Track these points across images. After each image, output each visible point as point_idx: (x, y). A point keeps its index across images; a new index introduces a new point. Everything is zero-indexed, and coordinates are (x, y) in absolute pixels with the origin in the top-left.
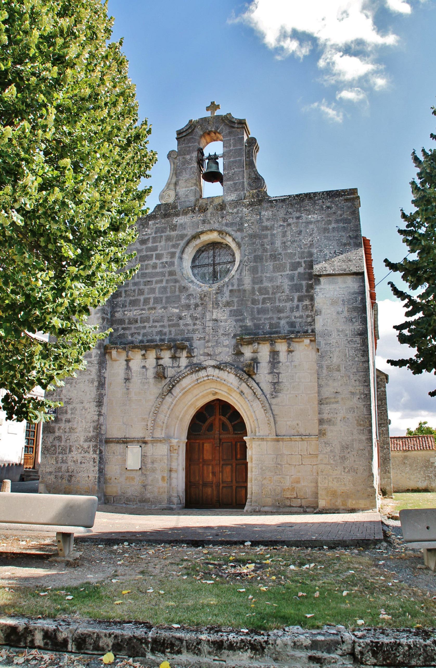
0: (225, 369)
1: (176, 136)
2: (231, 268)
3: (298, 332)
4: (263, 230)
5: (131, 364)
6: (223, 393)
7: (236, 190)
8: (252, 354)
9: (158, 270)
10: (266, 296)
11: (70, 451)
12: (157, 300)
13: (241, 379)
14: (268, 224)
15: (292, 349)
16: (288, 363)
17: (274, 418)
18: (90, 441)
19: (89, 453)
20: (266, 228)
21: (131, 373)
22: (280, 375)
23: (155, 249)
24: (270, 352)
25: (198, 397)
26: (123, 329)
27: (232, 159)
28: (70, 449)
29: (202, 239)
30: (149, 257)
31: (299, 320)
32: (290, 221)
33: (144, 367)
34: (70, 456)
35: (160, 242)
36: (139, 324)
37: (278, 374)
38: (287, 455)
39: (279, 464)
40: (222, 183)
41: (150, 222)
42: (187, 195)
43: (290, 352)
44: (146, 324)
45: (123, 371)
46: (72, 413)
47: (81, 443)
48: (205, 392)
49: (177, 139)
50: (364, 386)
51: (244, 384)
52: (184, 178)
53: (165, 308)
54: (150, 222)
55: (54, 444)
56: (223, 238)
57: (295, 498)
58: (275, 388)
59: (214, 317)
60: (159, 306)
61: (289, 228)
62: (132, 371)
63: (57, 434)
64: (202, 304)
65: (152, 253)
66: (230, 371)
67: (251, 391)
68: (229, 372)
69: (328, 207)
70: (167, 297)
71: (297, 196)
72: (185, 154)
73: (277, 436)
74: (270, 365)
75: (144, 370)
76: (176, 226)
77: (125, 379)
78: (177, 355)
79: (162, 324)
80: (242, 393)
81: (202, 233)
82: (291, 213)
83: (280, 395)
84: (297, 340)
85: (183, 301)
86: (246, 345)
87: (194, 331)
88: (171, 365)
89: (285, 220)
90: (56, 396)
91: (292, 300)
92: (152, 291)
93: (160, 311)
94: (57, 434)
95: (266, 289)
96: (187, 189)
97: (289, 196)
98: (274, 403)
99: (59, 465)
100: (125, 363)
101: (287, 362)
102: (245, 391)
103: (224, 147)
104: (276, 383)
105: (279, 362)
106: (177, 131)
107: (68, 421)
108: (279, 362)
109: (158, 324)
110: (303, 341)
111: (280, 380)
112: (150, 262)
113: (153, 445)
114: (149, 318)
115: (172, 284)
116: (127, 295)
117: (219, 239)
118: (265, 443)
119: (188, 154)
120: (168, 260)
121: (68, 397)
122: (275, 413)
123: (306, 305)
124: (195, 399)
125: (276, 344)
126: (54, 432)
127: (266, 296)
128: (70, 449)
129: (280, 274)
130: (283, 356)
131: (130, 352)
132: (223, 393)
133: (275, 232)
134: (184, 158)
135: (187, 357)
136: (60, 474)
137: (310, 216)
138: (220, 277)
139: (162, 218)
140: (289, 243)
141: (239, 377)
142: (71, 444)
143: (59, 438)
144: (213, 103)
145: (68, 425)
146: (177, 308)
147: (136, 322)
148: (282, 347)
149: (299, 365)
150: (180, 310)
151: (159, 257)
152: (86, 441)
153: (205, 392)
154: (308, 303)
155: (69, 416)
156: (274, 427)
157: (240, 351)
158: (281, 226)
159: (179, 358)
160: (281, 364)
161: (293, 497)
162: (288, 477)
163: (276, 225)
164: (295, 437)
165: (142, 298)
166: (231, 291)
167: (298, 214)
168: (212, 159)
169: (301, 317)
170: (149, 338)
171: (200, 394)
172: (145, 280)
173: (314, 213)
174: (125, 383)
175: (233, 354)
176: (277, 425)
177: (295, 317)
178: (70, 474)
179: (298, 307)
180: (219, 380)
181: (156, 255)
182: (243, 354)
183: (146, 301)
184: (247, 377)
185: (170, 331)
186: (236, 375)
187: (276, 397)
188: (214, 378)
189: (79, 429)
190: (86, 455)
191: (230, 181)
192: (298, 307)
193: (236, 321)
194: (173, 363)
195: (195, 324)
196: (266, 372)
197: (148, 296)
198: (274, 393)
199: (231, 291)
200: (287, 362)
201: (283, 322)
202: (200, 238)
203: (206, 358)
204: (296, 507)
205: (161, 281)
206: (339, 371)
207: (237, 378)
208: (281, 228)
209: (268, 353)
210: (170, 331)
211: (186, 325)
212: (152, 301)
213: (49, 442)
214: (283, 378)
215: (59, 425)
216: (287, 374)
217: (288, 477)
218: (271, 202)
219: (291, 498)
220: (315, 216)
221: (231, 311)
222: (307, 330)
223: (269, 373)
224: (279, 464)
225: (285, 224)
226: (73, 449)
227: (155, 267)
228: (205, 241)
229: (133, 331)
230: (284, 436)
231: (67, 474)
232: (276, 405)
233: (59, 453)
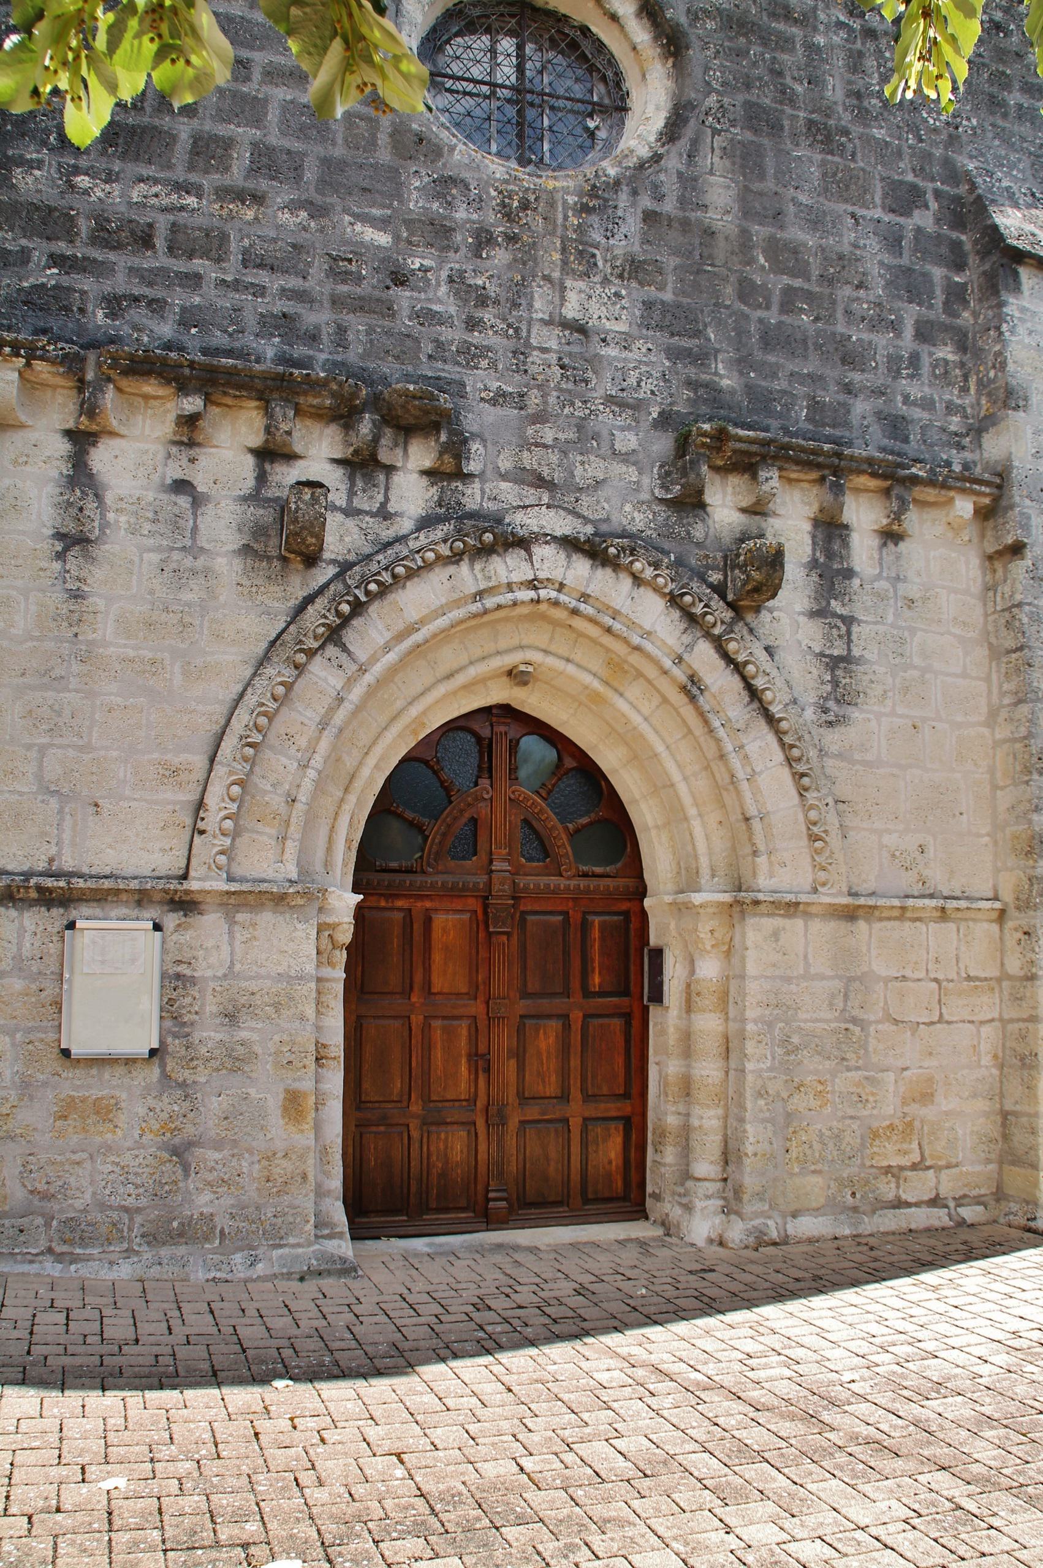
22: (855, 629)
31: (917, 413)
37: (849, 621)
38: (887, 980)
39: (854, 1021)
43: (891, 536)
57: (914, 1167)
58: (835, 683)
83: (855, 714)
91: (895, 327)
105: (849, 574)
127: (797, 283)
130: (863, 549)
148: (863, 514)
160: (856, 582)
161: (905, 1161)
162: (890, 1077)
177: (906, 399)
179: (914, 360)
196: (798, 608)
198: (831, 704)
204: (917, 1205)
216: (881, 628)
217: (890, 1077)
219: (902, 1168)
223: (813, 614)
230: (873, 894)
232: (840, 756)
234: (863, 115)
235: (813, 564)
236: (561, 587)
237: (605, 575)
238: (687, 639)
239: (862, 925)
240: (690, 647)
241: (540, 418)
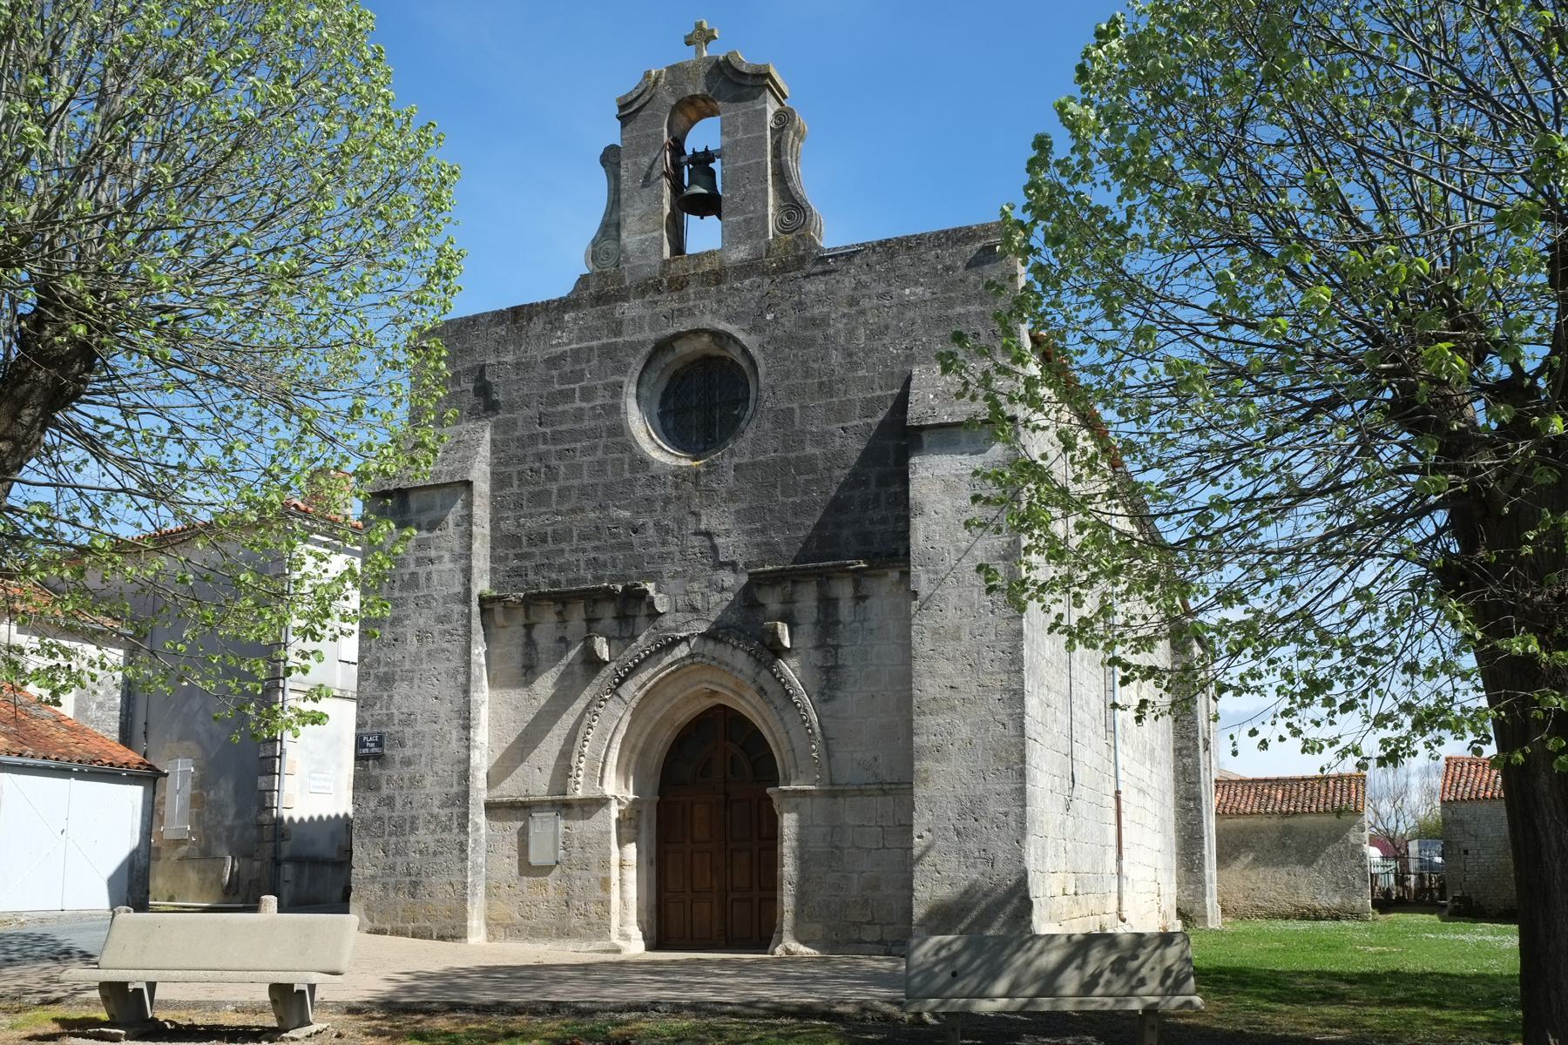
3: (877, 554)
4: (805, 328)
5: (536, 634)
7: (749, 236)
9: (587, 424)
10: (811, 477)
11: (414, 829)
12: (584, 492)
13: (759, 661)
14: (817, 311)
15: (864, 592)
20: (813, 323)
23: (579, 375)
24: (819, 600)
26: (517, 556)
27: (740, 164)
28: (413, 823)
30: (568, 396)
32: (865, 303)
33: (562, 639)
36: (550, 546)
37: (837, 647)
41: (566, 317)
42: (643, 252)
43: (860, 598)
44: (563, 545)
48: (690, 691)
51: (765, 672)
53: (603, 507)
54: (566, 317)
56: (722, 348)
57: (868, 923)
58: (829, 680)
59: (703, 527)
60: (588, 504)
61: (862, 320)
63: (385, 791)
64: (679, 498)
67: (779, 687)
68: (735, 648)
69: (947, 269)
70: (605, 485)
71: (880, 244)
73: (832, 784)
76: (621, 323)
78: (629, 612)
80: (761, 691)
81: (678, 336)
82: (866, 286)
83: (839, 694)
85: (639, 492)
87: (663, 557)
89: (853, 302)
91: (865, 483)
92: (575, 470)
93: (592, 515)
94: (385, 791)
95: (810, 460)
100: (523, 631)
102: (767, 688)
103: (723, 133)
105: (838, 622)
106: (619, 100)
107: (407, 762)
108: (838, 622)
109: (588, 545)
112: (567, 407)
117: (715, 351)
121: (404, 710)
124: (668, 706)
125: (832, 582)
126: (378, 789)
127: (811, 477)
128: (413, 823)
130: (845, 610)
131: (532, 609)
133: (831, 331)
137: (907, 291)
143: (389, 802)
144: (699, 26)
145: (407, 772)
146: (625, 508)
147: (544, 540)
148: (843, 590)
151: (587, 394)
152: (441, 807)
153: (690, 691)
155: (408, 752)
158: (844, 315)
159: (634, 617)
162: (855, 876)
165: (554, 487)
166: (737, 468)
169: (884, 521)
170: (571, 575)
172: (559, 447)
173: (917, 283)
177: (872, 522)
181: (582, 388)
183: (563, 493)
184: (770, 656)
185: (614, 560)
186: (749, 653)
189: (429, 780)
190: (445, 835)
193: (750, 533)
195: (664, 544)
197: (568, 483)
199: (737, 468)
201: (846, 533)
202: (673, 349)
203: (689, 616)
205: (594, 448)
206: (959, 639)
210: (614, 560)
211: (647, 545)
212: (575, 494)
214: (847, 655)
215: (388, 772)
217: (855, 876)
218: (823, 260)
220: (919, 290)
221: (737, 512)
222: (897, 550)
223: (817, 648)
227: (579, 415)
232: (830, 716)
233: (390, 835)
234: (854, 366)
235: (818, 622)
237: (720, 647)
239: (840, 800)
241: (692, 580)
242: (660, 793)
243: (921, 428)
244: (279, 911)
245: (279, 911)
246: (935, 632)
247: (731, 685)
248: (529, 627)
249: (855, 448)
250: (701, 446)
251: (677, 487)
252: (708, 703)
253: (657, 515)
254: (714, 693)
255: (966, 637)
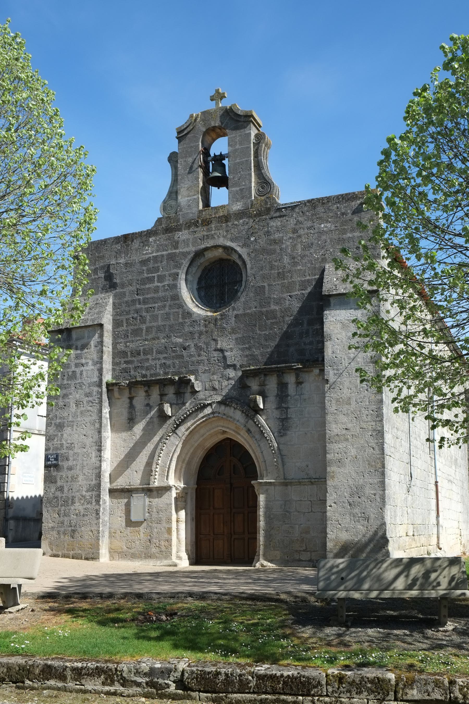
0: (230, 404)
1: (176, 135)
2: (239, 289)
3: (308, 361)
4: (271, 245)
5: (134, 402)
6: (231, 432)
7: (242, 198)
8: (259, 387)
9: (161, 294)
11: (73, 503)
12: (159, 329)
13: (247, 415)
14: (277, 236)
15: (301, 380)
16: (297, 397)
17: (282, 459)
18: (93, 490)
19: (91, 504)
20: (275, 242)
21: (135, 412)
22: (289, 410)
23: (157, 270)
25: (205, 436)
26: (125, 362)
27: (238, 161)
28: (73, 500)
29: (206, 256)
30: (151, 280)
31: (308, 347)
32: (301, 232)
33: (148, 405)
34: (72, 508)
35: (161, 262)
36: (142, 357)
37: (287, 408)
38: (296, 501)
39: (287, 511)
40: (227, 188)
41: (151, 240)
42: (189, 206)
43: (299, 383)
44: (149, 356)
45: (127, 410)
46: (74, 460)
47: (84, 493)
48: (212, 431)
49: (177, 138)
50: (375, 421)
51: (250, 421)
52: (186, 186)
53: (168, 337)
54: (151, 240)
55: (56, 495)
56: (229, 255)
57: (304, 551)
58: (283, 425)
59: (219, 347)
60: (161, 335)
61: (299, 240)
62: (136, 410)
63: (59, 483)
64: (207, 332)
65: (153, 275)
66: (235, 407)
67: (258, 429)
68: (235, 409)
69: (343, 214)
70: (169, 325)
71: (309, 201)
72: (186, 157)
73: (285, 479)
74: (278, 399)
75: (148, 408)
76: (177, 243)
77: (129, 419)
78: (182, 391)
79: (165, 355)
80: (249, 431)
81: (206, 249)
82: (301, 223)
83: (289, 433)
84: (305, 370)
85: (187, 329)
86: (253, 377)
87: (199, 362)
88: (175, 403)
89: (295, 231)
90: (57, 441)
92: (155, 318)
94: (59, 483)
95: (273, 312)
96: (189, 198)
97: (300, 202)
98: (282, 442)
99: (62, 519)
100: (128, 401)
101: (296, 395)
102: (251, 429)
103: (229, 145)
104: (285, 419)
105: (288, 396)
106: (177, 129)
107: (70, 469)
108: (288, 396)
109: (161, 356)
110: (312, 371)
111: (289, 416)
112: (151, 285)
113: (158, 493)
114: (152, 349)
115: (175, 310)
116: (128, 324)
117: (225, 256)
118: (273, 487)
119: (190, 156)
120: (171, 282)
121: (69, 442)
122: (283, 453)
123: (317, 329)
124: (201, 439)
125: (284, 375)
126: (56, 482)
127: (274, 320)
128: (73, 500)
129: (289, 294)
130: (291, 389)
131: (133, 389)
132: (231, 432)
133: (284, 246)
134: (185, 161)
135: (190, 392)
136: (63, 529)
137: (322, 226)
138: (228, 299)
139: (163, 234)
140: (299, 258)
141: (245, 413)
142: (73, 494)
143: (61, 489)
144: (217, 91)
145: (70, 474)
146: (179, 337)
147: (139, 354)
148: (291, 379)
149: (309, 398)
150: (184, 339)
151: (161, 279)
152: (87, 491)
153: (212, 431)
154: (318, 327)
155: (70, 463)
156: (281, 470)
157: (246, 384)
158: (290, 238)
160: (289, 397)
161: (302, 549)
162: (297, 526)
163: (285, 238)
164: (304, 480)
165: (144, 327)
166: (236, 316)
167: (309, 224)
168: (217, 160)
169: (311, 343)
170: (152, 372)
171: (207, 434)
172: (146, 306)
173: (327, 222)
174: (129, 423)
175: (240, 388)
176: (285, 466)
177: (305, 344)
178: (73, 528)
179: (307, 332)
180: (224, 417)
181: (158, 276)
182: (250, 387)
183: (148, 330)
184: (253, 413)
185: (174, 364)
186: (243, 412)
187: (285, 435)
188: (220, 415)
189: (81, 478)
190: (89, 506)
191: (236, 186)
192: (307, 332)
193: (243, 350)
194: (177, 400)
195: (199, 355)
196: (273, 407)
197: (151, 325)
198: (282, 431)
199: (236, 316)
200: (296, 395)
201: (292, 349)
202: (204, 256)
203: (212, 393)
204: (305, 561)
205: (164, 306)
206: (350, 404)
207: (244, 415)
208: (291, 241)
209: (276, 386)
210: (174, 364)
211: (191, 356)
212: (154, 330)
213: (51, 494)
214: (292, 413)
215: (61, 474)
216: (296, 409)
218: (279, 210)
219: (301, 551)
220: (329, 225)
221: (236, 339)
222: (318, 358)
223: (277, 409)
224: (287, 511)
225: (295, 236)
226: (76, 500)
227: (156, 290)
228: (211, 258)
229: (136, 364)
230: (293, 479)
231: (70, 529)
232: (284, 444)
233: (61, 506)
234: (295, 264)
235: (277, 395)
236: (219, 413)
237: (228, 408)
238: (246, 420)
239: (289, 487)
240: (247, 422)
242: (198, 483)
243: (330, 296)
244: (7, 547)
245: (7, 547)
246: (337, 400)
247: (233, 428)
248: (131, 399)
249: (296, 305)
250: (218, 305)
251: (206, 326)
252: (221, 437)
253: (196, 341)
254: (224, 432)
255: (353, 403)
